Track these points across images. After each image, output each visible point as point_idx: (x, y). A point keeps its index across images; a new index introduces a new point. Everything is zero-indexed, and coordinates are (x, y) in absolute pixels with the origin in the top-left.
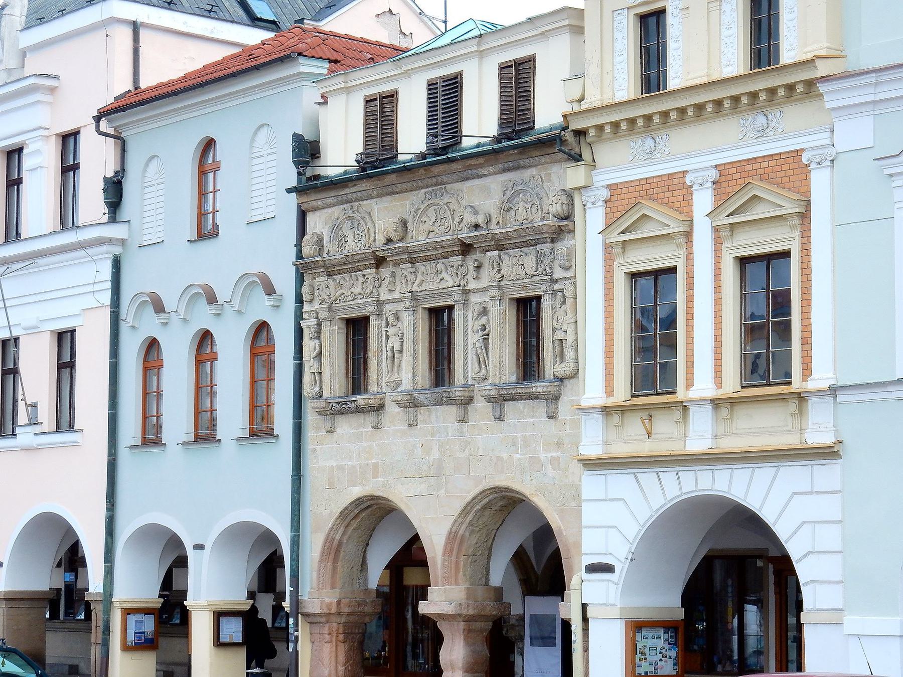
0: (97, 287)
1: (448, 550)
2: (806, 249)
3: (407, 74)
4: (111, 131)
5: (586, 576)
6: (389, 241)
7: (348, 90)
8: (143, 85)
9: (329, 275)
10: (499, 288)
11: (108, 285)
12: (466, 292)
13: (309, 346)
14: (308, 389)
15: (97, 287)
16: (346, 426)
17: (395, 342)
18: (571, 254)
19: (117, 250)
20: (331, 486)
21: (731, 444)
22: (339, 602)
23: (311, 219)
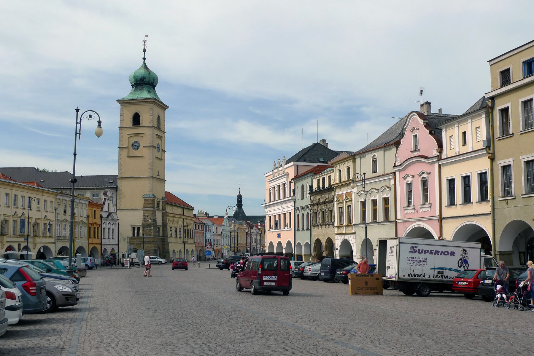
0: (292, 206)
1: (325, 247)
2: (352, 205)
3: (320, 177)
4: (294, 182)
5: (336, 250)
6: (318, 201)
7: (315, 178)
8: (299, 174)
9: (313, 206)
10: (328, 208)
11: (294, 206)
12: (325, 209)
13: (311, 216)
14: (311, 223)
15: (292, 206)
16: (316, 228)
17: (319, 216)
18: (333, 204)
19: (295, 200)
20: (314, 237)
21: (347, 232)
22: (316, 254)
23: (311, 197)
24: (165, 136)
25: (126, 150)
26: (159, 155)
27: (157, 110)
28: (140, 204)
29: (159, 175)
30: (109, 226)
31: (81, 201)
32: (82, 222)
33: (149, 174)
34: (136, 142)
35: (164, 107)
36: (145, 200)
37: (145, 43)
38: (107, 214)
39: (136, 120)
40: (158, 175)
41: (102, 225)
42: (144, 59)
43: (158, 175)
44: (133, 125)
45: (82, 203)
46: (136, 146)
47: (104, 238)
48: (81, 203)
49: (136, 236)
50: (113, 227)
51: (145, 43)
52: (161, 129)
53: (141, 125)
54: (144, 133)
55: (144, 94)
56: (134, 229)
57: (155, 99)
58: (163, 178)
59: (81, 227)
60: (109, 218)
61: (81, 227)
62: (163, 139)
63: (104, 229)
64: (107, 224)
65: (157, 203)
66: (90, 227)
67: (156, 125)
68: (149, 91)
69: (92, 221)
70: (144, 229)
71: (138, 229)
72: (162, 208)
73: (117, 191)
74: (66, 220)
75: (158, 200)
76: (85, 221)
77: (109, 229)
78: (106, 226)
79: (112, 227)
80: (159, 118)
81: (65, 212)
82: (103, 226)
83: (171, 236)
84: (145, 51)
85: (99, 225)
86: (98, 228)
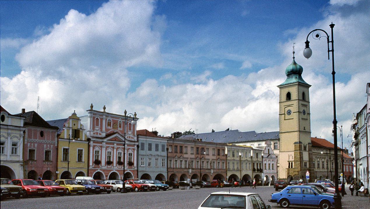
24: (309, 104)
25: (284, 115)
26: (305, 117)
27: (302, 89)
28: (292, 147)
29: (305, 129)
30: (270, 162)
31: (245, 149)
32: (247, 160)
33: (297, 129)
34: (289, 110)
35: (308, 86)
36: (295, 146)
37: (294, 48)
38: (267, 155)
39: (289, 96)
40: (304, 129)
41: (264, 161)
42: (294, 58)
43: (304, 129)
44: (287, 100)
45: (247, 150)
46: (289, 113)
47: (265, 169)
48: (245, 150)
49: (290, 168)
50: (273, 162)
51: (294, 48)
52: (307, 100)
53: (291, 100)
54: (293, 105)
55: (294, 80)
56: (289, 163)
57: (299, 82)
58: (308, 131)
59: (246, 163)
60: (269, 157)
61: (246, 163)
62: (307, 106)
63: (265, 164)
64: (271, 161)
65: (304, 147)
66: (254, 164)
67: (301, 98)
68: (296, 78)
69: (255, 159)
70: (294, 163)
71: (292, 163)
72: (309, 150)
73: (279, 141)
74: (234, 160)
75: (305, 145)
76: (250, 159)
77: (269, 164)
78: (266, 162)
79: (273, 162)
80: (304, 94)
81: (233, 156)
82: (264, 163)
83: (318, 167)
84: (294, 53)
85: (261, 162)
86: (260, 164)
